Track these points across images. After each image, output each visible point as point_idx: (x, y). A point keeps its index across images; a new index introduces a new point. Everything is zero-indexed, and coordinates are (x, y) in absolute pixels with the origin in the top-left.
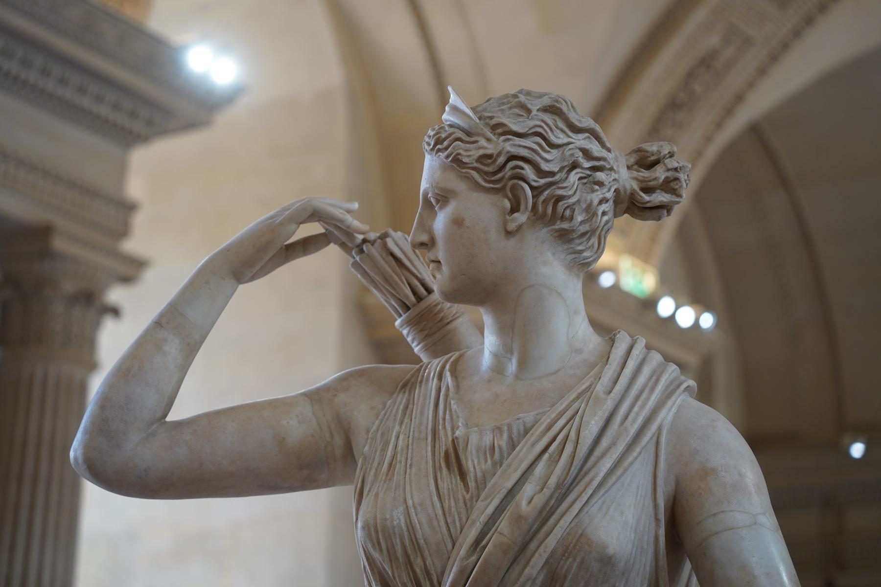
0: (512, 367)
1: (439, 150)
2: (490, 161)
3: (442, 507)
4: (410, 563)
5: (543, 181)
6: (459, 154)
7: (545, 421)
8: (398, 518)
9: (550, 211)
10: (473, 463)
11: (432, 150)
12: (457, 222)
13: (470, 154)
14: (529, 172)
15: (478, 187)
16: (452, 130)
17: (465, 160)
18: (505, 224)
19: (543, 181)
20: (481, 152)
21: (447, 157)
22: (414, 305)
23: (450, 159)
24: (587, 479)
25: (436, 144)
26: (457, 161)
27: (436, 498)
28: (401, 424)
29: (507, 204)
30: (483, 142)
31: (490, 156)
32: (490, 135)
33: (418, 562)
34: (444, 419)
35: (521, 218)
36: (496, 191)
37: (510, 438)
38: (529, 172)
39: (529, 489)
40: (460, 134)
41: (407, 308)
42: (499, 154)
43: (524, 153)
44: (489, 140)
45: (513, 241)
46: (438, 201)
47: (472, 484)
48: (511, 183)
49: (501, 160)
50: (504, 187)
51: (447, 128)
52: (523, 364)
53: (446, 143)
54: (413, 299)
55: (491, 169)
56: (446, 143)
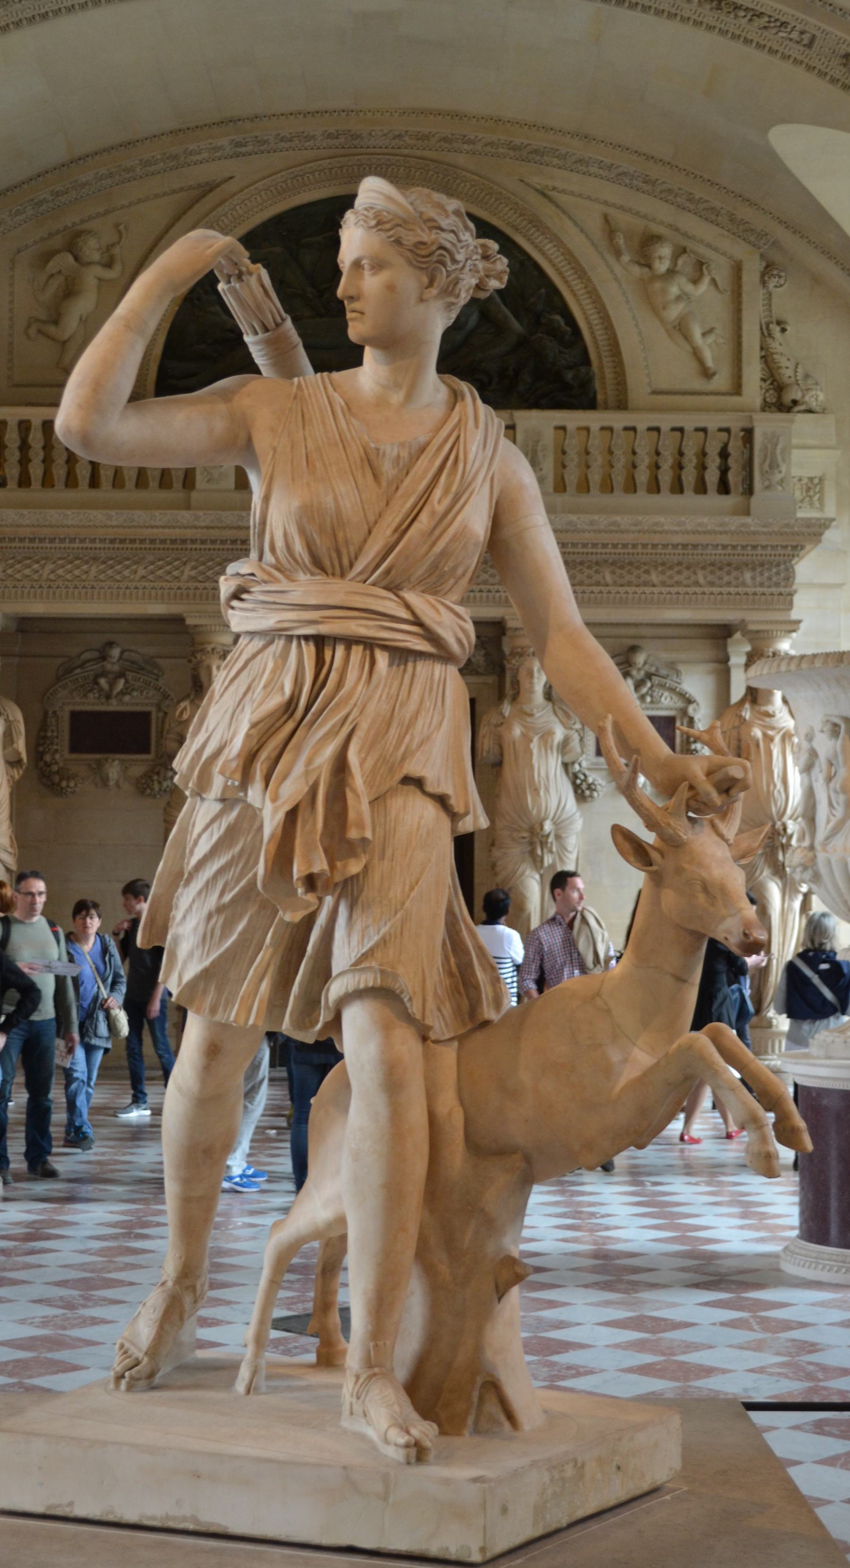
0: (397, 398)
1: (380, 230)
2: (423, 247)
3: (360, 497)
4: (335, 535)
5: (454, 267)
6: (400, 237)
7: (436, 443)
8: (329, 501)
9: (450, 289)
10: (387, 469)
11: (372, 227)
12: (391, 288)
13: (410, 239)
14: (448, 260)
15: (410, 263)
16: (390, 217)
17: (405, 242)
18: (422, 294)
19: (454, 267)
20: (418, 239)
21: (389, 237)
22: (274, 329)
23: (392, 239)
24: (471, 489)
25: (379, 223)
26: (398, 242)
27: (356, 492)
28: (304, 428)
29: (426, 280)
30: (419, 231)
31: (424, 243)
32: (424, 226)
33: (340, 535)
34: (350, 431)
35: (434, 291)
36: (422, 269)
37: (410, 453)
38: (448, 260)
39: (438, 493)
40: (400, 222)
41: (266, 329)
42: (432, 244)
43: (448, 245)
44: (423, 230)
45: (422, 307)
46: (372, 268)
47: (384, 484)
48: (433, 266)
49: (434, 247)
50: (427, 268)
51: (385, 214)
52: (409, 397)
53: (388, 226)
54: (273, 325)
55: (423, 253)
56: (388, 226)
